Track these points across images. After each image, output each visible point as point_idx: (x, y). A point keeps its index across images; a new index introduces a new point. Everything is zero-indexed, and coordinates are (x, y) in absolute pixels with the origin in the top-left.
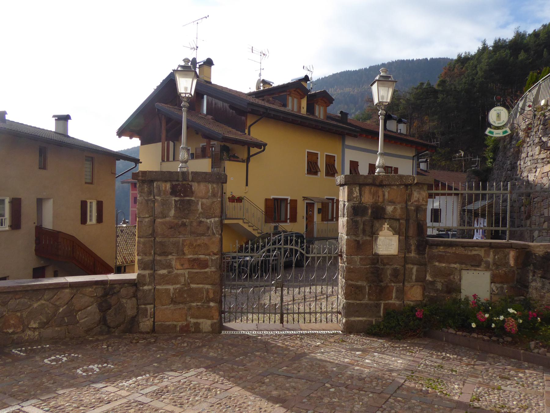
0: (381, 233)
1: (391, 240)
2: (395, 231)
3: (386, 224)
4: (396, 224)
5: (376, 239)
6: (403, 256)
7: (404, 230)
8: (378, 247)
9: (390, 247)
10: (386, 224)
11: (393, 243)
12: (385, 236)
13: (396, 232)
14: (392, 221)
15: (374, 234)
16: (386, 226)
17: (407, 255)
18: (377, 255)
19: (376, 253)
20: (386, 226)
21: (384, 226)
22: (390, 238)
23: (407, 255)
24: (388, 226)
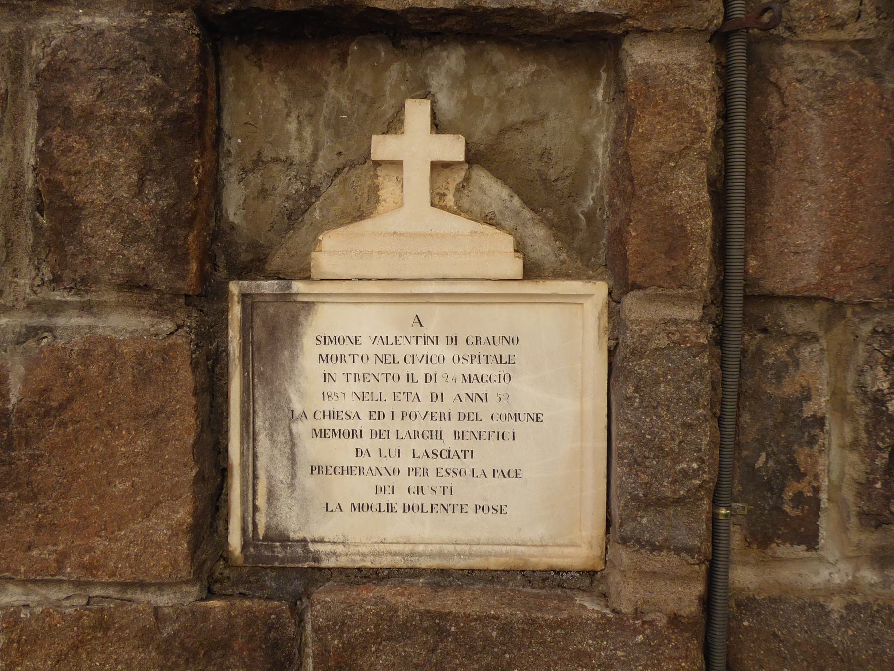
0: (335, 250)
1: (499, 352)
2: (563, 228)
3: (417, 113)
4: (571, 118)
5: (274, 333)
6: (686, 597)
7: (689, 189)
8: (313, 450)
9: (489, 455)
10: (417, 113)
11: (526, 393)
12: (397, 290)
13: (575, 228)
14: (519, 73)
15: (220, 274)
16: (416, 144)
17: (744, 576)
18: (291, 573)
19: (268, 543)
20: (416, 144)
21: (383, 147)
22: (495, 320)
23: (744, 576)
24: (452, 148)
